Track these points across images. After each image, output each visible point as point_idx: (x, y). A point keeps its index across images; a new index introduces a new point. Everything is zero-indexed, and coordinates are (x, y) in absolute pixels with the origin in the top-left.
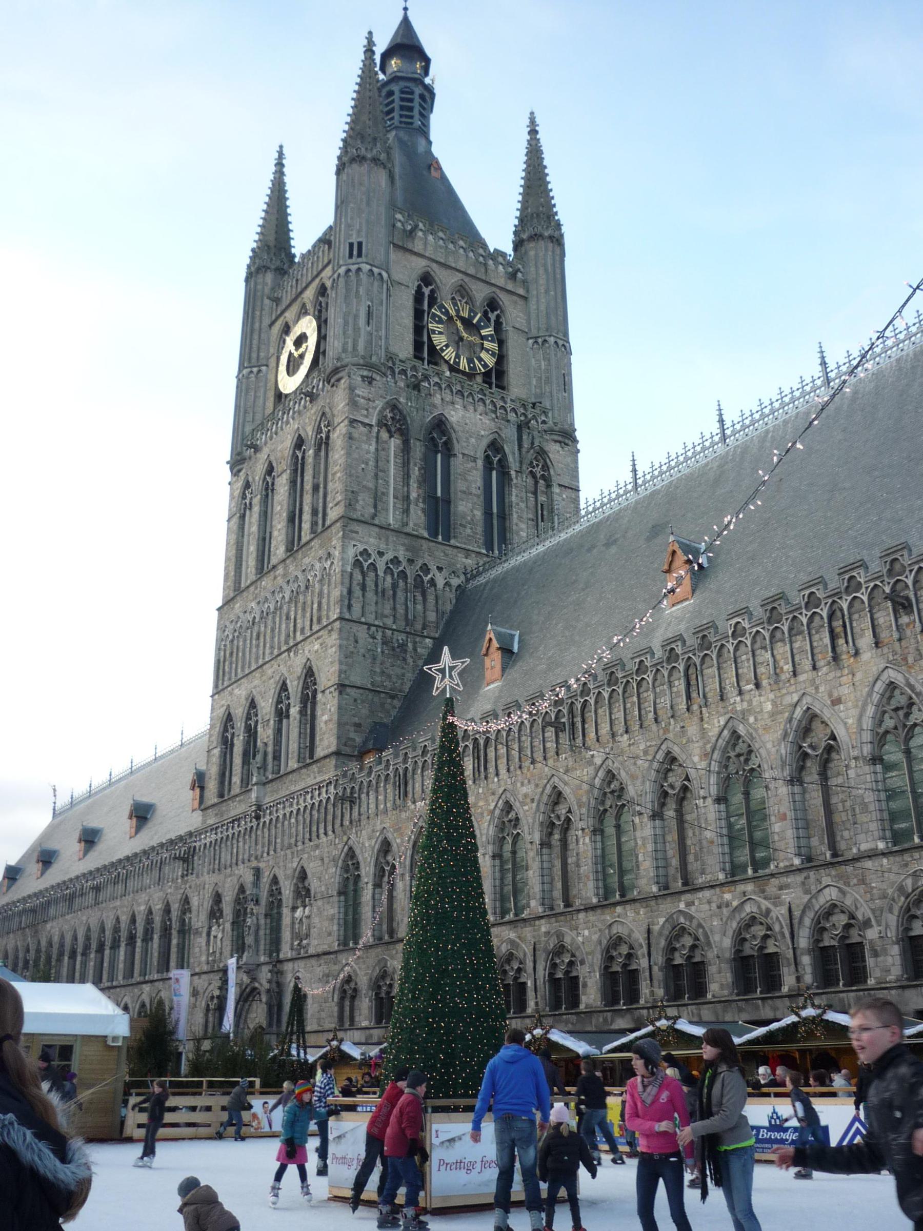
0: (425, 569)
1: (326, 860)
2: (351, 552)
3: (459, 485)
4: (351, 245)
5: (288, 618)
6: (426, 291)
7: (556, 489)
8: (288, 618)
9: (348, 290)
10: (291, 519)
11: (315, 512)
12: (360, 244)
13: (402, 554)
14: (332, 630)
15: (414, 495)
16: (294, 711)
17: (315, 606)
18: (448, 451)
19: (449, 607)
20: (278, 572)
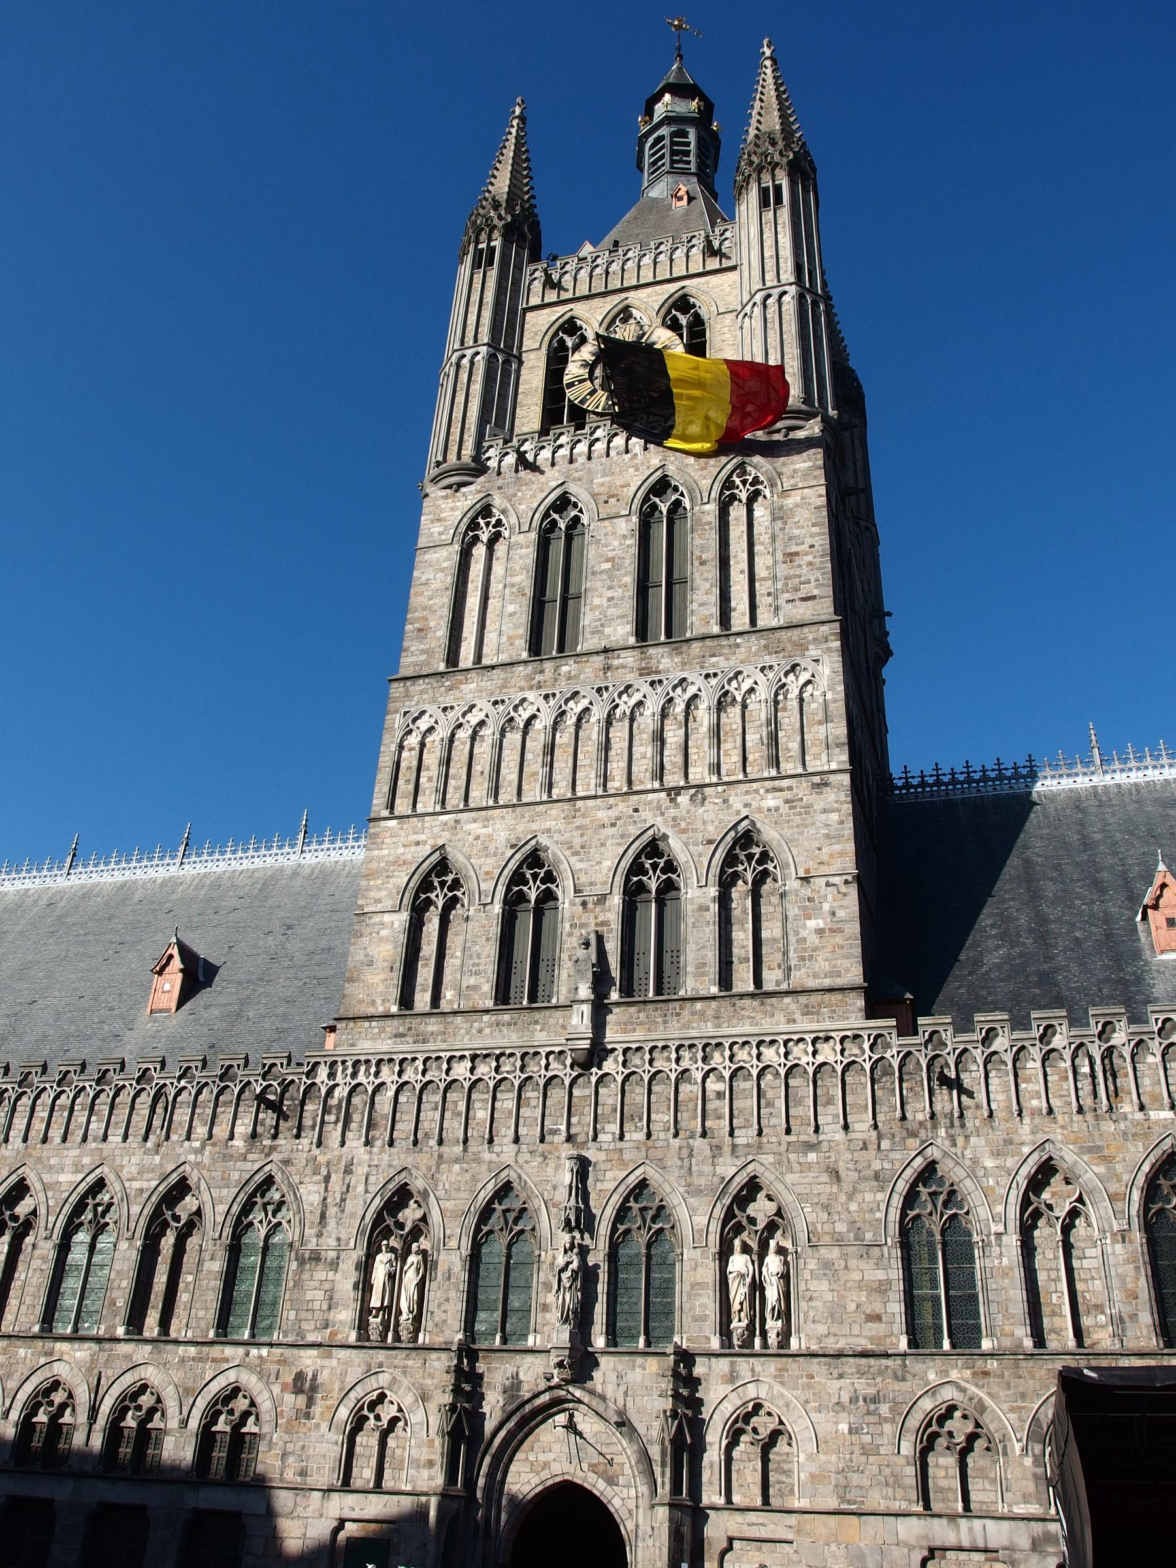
1: (849, 1177)
5: (659, 738)
14: (826, 784)
20: (616, 662)
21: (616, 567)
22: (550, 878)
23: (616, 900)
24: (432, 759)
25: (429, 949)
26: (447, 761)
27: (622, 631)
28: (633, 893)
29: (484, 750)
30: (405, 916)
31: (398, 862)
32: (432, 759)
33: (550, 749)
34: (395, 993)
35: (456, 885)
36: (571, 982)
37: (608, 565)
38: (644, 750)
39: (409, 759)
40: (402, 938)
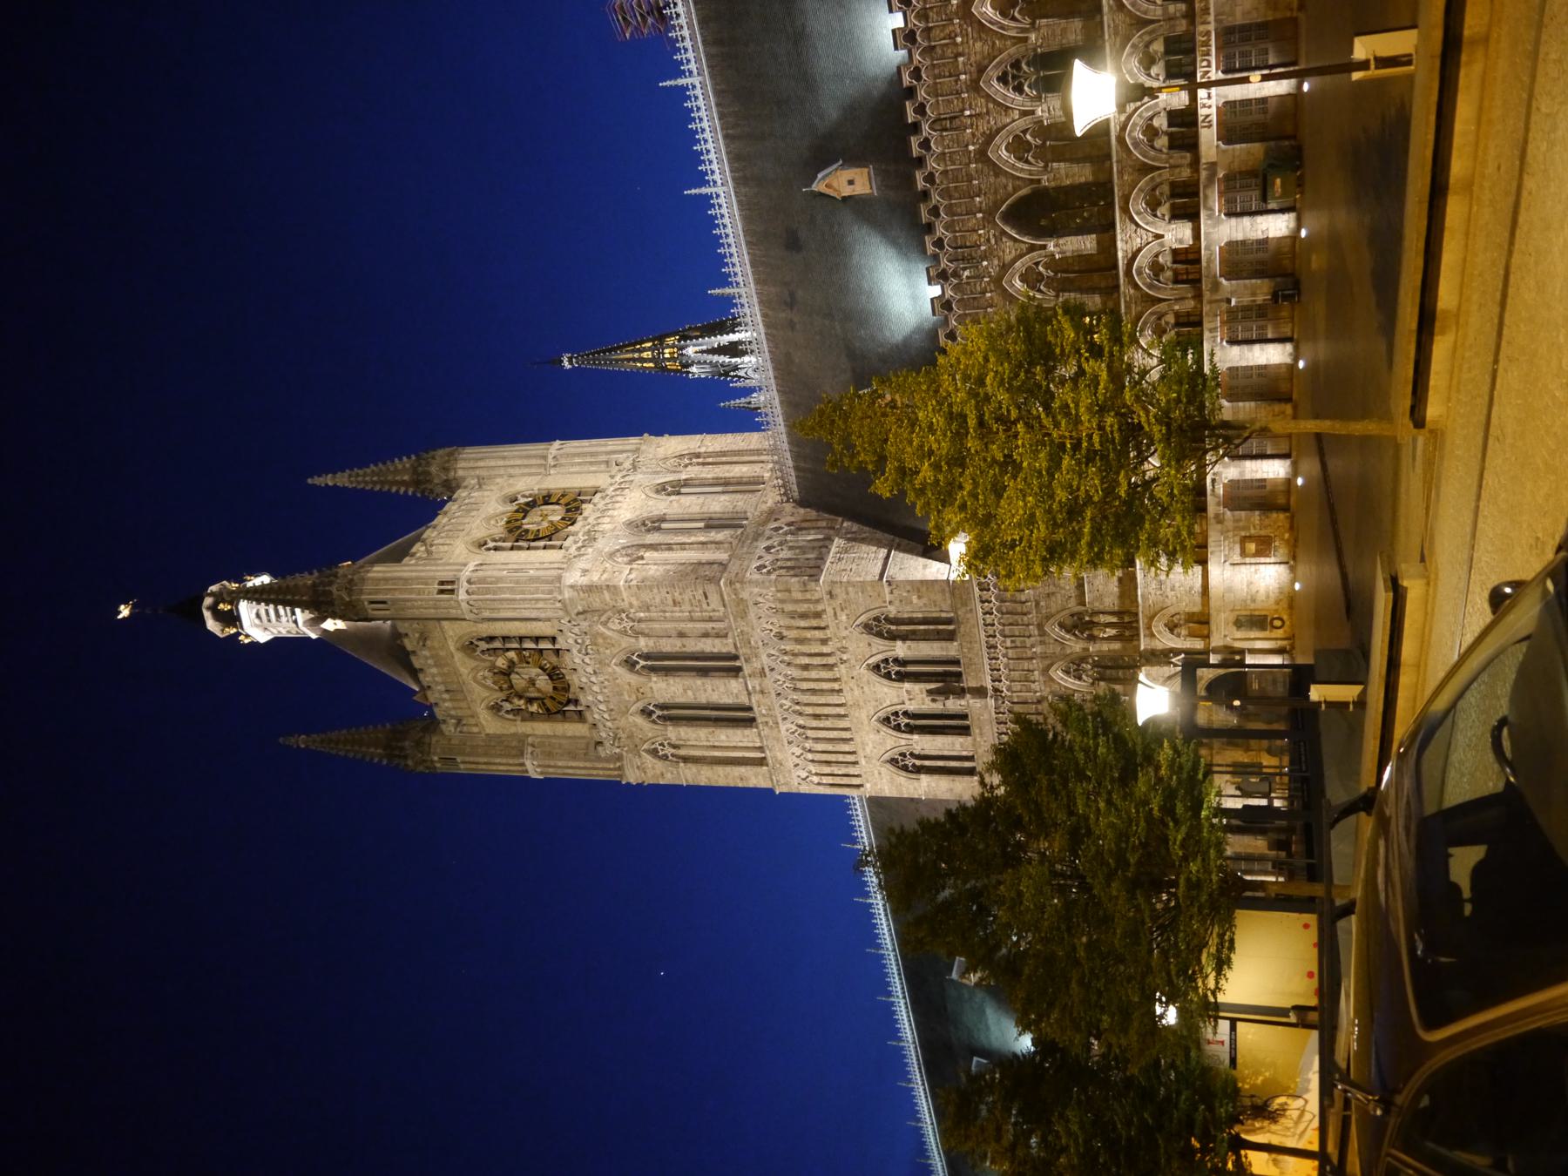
0: (777, 529)
2: (756, 576)
3: (696, 509)
4: (442, 592)
5: (806, 667)
6: (491, 544)
7: (703, 450)
8: (806, 667)
9: (488, 591)
10: (704, 672)
11: (706, 635)
12: (442, 583)
13: (763, 544)
15: (702, 539)
16: (901, 649)
17: (803, 623)
18: (663, 519)
19: (813, 514)
21: (690, 688)
22: (896, 714)
23: (907, 685)
24: (827, 770)
25: (940, 763)
26: (828, 763)
27: (735, 685)
28: (902, 677)
29: (820, 747)
30: (923, 777)
31: (892, 781)
32: (827, 770)
33: (817, 717)
34: (967, 778)
35: (903, 755)
36: (953, 705)
37: (690, 693)
38: (814, 674)
39: (830, 780)
40: (936, 777)
